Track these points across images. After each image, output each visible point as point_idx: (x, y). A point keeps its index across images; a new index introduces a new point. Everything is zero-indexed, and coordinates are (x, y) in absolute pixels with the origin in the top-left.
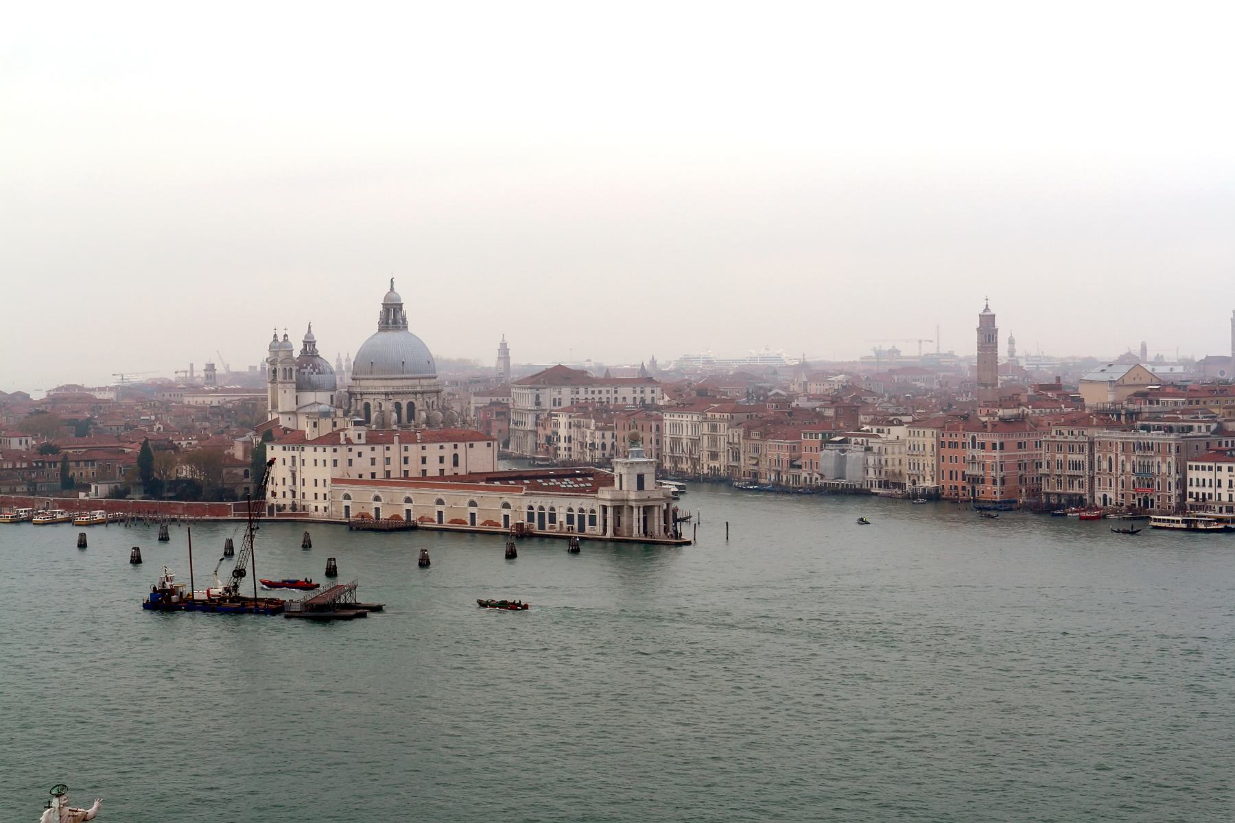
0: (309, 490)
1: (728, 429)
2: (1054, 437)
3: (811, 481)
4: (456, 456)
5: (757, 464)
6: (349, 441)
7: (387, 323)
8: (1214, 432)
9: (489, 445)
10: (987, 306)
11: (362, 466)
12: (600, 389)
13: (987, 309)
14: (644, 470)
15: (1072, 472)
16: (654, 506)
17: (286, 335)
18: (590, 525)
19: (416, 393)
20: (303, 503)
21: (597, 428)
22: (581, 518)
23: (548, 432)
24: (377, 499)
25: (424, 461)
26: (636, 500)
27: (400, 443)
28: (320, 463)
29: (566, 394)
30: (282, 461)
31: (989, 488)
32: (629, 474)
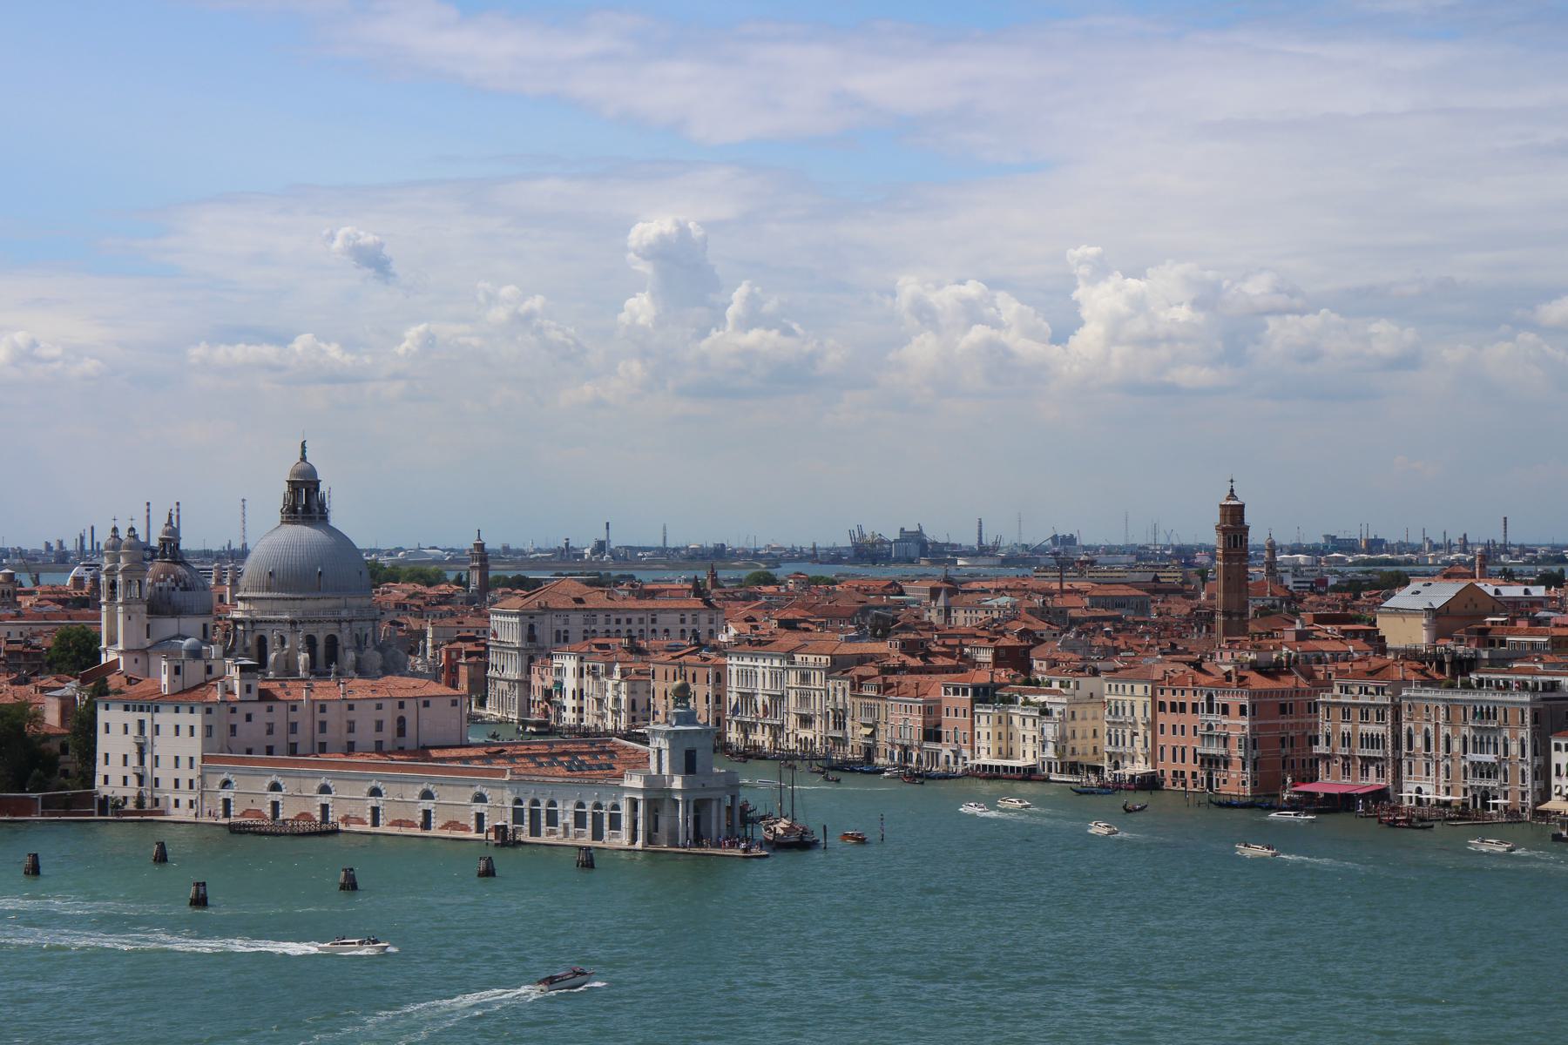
0: (165, 773)
1: (826, 678)
2: (1338, 697)
3: (956, 763)
4: (401, 720)
5: (872, 735)
7: (295, 511)
10: (1232, 491)
13: (1232, 495)
15: (1367, 752)
16: (711, 800)
17: (132, 529)
18: (610, 829)
20: (156, 795)
22: (597, 819)
23: (549, 683)
24: (275, 787)
28: (184, 731)
30: (122, 728)
31: (1234, 776)
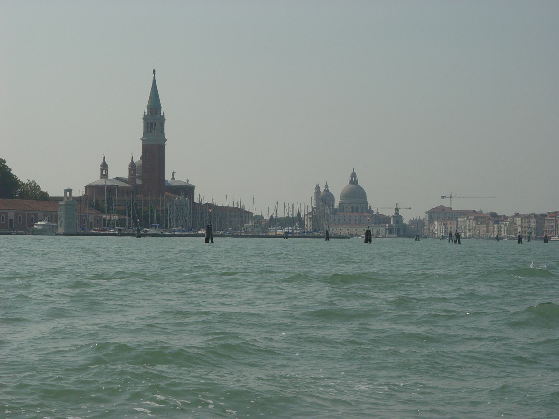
1: (473, 221)
5: (479, 233)
23: (433, 228)
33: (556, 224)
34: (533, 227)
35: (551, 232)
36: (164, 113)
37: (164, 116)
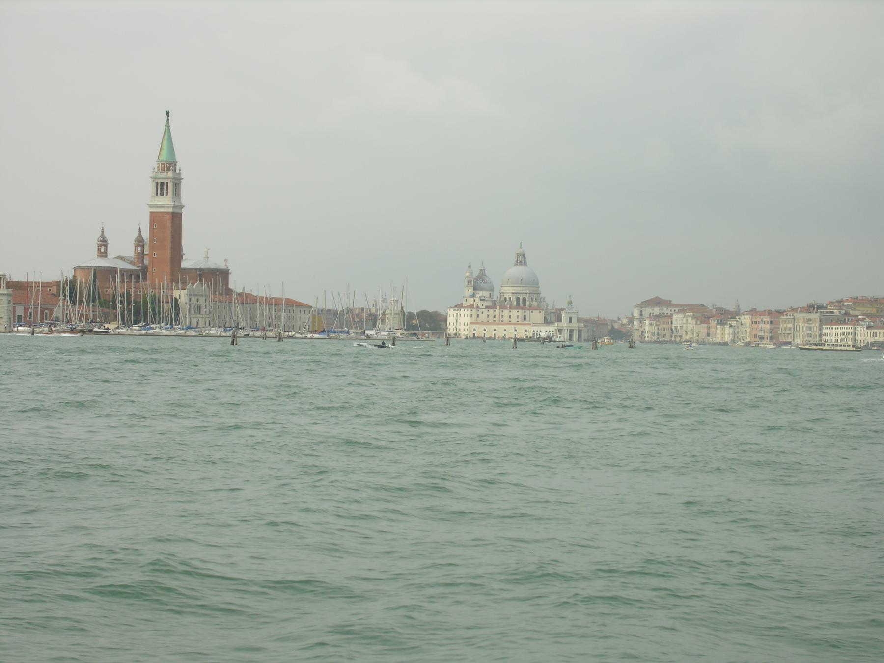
0: (462, 327)
4: (525, 316)
6: (478, 307)
8: (843, 315)
9: (540, 312)
11: (483, 317)
12: (675, 309)
14: (572, 315)
16: (574, 330)
19: (526, 293)
20: (460, 333)
21: (656, 325)
24: (485, 330)
25: (510, 317)
26: (566, 327)
27: (500, 309)
28: (466, 316)
29: (657, 311)
32: (566, 317)
33: (794, 325)
34: (766, 329)
35: (788, 337)
36: (180, 170)
37: (180, 174)
